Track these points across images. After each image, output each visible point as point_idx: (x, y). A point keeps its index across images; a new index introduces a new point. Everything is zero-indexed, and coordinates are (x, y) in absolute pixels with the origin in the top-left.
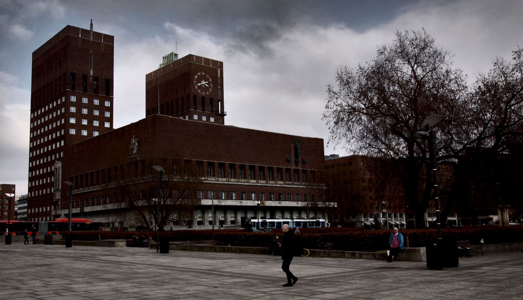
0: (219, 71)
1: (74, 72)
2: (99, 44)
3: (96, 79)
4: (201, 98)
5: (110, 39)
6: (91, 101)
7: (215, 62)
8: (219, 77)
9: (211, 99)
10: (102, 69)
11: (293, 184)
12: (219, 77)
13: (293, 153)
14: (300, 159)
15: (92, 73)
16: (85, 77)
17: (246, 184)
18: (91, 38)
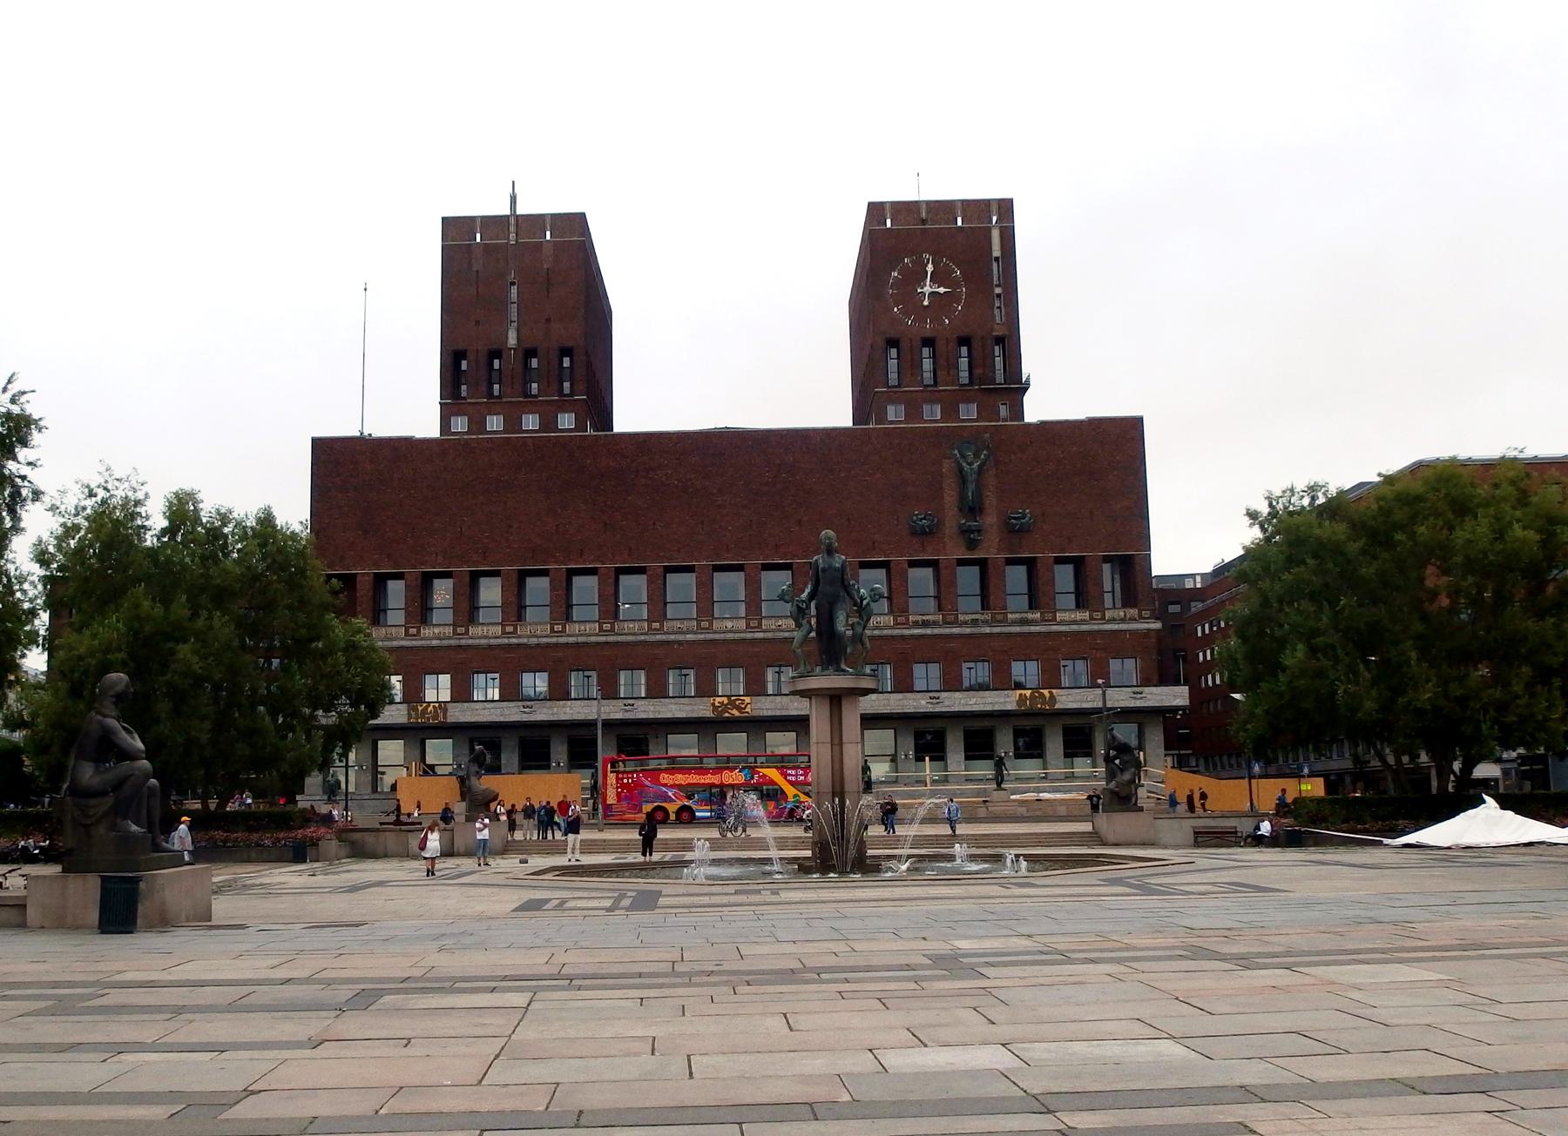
0: (995, 234)
1: (460, 347)
2: (539, 247)
5: (575, 225)
7: (978, 209)
8: (996, 253)
10: (548, 320)
11: (946, 623)
12: (996, 253)
13: (950, 497)
14: (990, 519)
15: (512, 340)
17: (690, 637)
18: (512, 236)
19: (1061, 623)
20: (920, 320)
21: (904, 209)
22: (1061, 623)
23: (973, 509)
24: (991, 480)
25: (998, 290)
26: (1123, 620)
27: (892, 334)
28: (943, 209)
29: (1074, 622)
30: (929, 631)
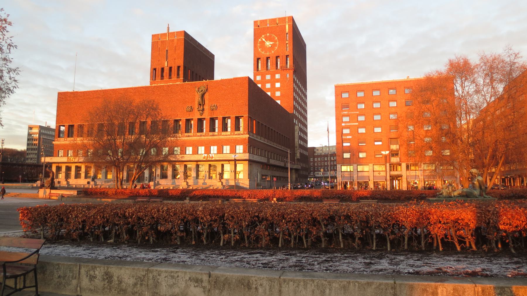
0: (287, 26)
3: (171, 68)
4: (265, 59)
14: (206, 107)
16: (163, 69)
19: (223, 135)
20: (266, 52)
21: (264, 22)
22: (223, 135)
23: (202, 104)
24: (206, 96)
25: (287, 42)
26: (239, 135)
27: (258, 57)
28: (273, 21)
29: (226, 135)
30: (188, 138)
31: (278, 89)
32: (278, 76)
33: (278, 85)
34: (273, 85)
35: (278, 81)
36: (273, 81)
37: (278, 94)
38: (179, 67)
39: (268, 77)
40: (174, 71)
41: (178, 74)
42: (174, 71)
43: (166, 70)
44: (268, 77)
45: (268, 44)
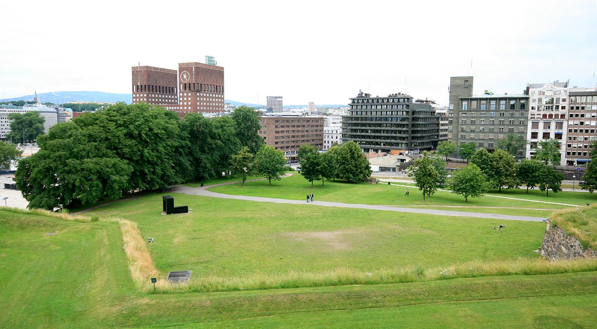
3: (142, 86)
6: (140, 95)
9: (190, 84)
16: (138, 86)
31: (190, 101)
32: (190, 94)
33: (190, 99)
34: (188, 99)
35: (190, 97)
36: (187, 97)
37: (190, 103)
38: (145, 86)
39: (185, 94)
40: (143, 87)
41: (145, 89)
42: (143, 87)
43: (139, 87)
44: (185, 94)
45: (185, 76)
